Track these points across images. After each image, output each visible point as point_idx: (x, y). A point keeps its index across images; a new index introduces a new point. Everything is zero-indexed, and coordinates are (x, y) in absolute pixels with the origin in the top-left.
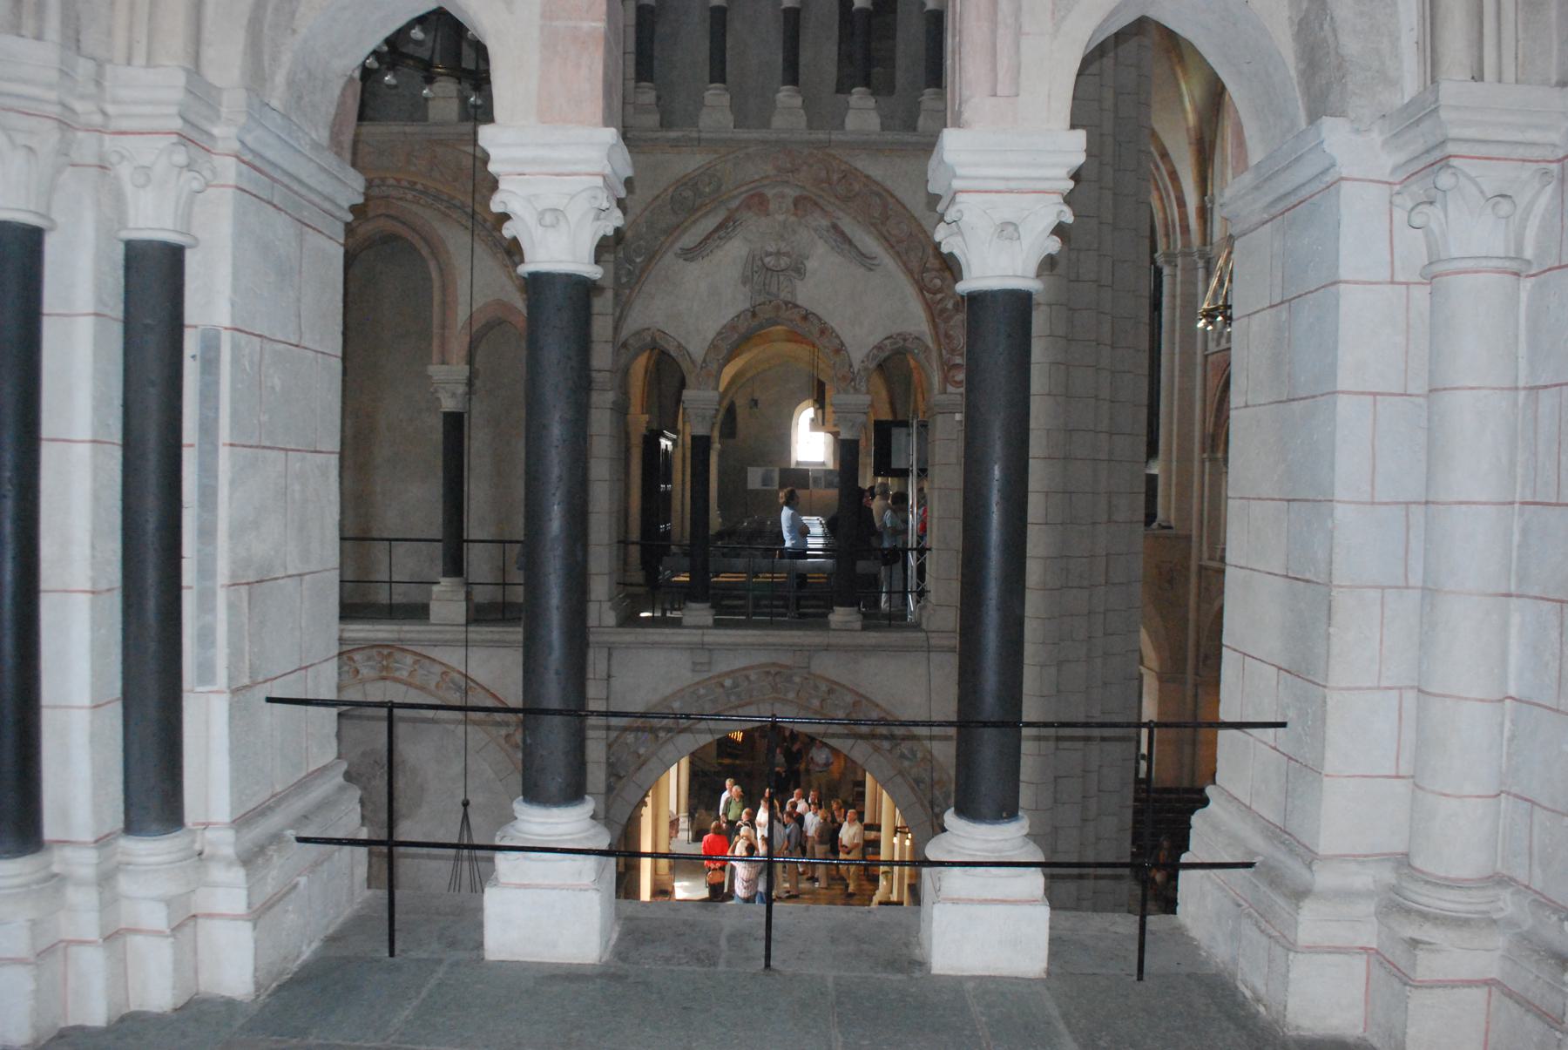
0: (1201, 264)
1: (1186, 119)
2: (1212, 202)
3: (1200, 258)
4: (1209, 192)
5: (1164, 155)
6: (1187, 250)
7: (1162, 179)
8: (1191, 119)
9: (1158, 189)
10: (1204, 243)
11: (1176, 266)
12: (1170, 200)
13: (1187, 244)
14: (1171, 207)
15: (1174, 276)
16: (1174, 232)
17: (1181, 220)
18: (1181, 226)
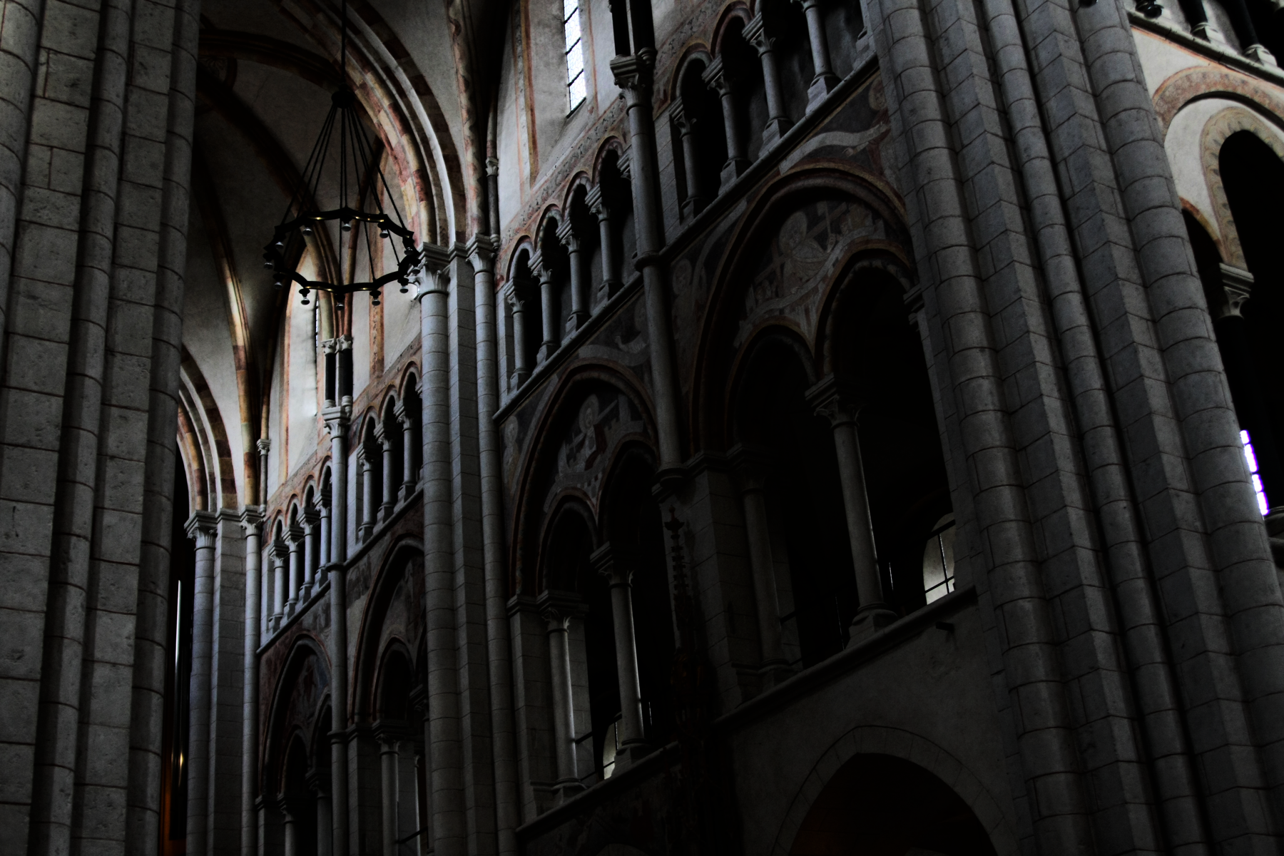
0: (251, 529)
1: (233, 333)
2: (267, 447)
3: (249, 521)
4: (263, 435)
5: (203, 388)
6: (230, 511)
7: (198, 419)
8: (241, 336)
9: (191, 430)
10: (256, 500)
11: (215, 535)
12: (208, 449)
13: (231, 503)
14: (209, 456)
15: (212, 549)
16: (214, 490)
17: (223, 472)
18: (223, 480)
